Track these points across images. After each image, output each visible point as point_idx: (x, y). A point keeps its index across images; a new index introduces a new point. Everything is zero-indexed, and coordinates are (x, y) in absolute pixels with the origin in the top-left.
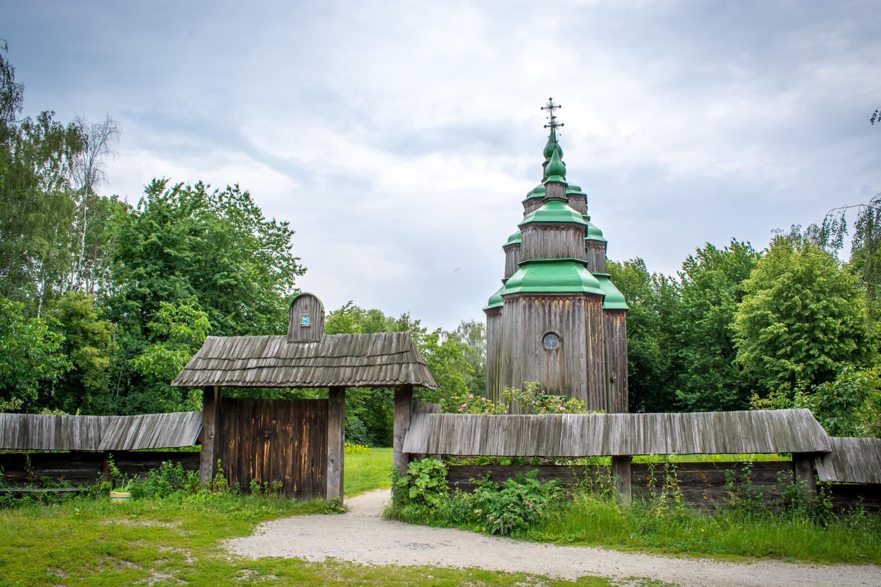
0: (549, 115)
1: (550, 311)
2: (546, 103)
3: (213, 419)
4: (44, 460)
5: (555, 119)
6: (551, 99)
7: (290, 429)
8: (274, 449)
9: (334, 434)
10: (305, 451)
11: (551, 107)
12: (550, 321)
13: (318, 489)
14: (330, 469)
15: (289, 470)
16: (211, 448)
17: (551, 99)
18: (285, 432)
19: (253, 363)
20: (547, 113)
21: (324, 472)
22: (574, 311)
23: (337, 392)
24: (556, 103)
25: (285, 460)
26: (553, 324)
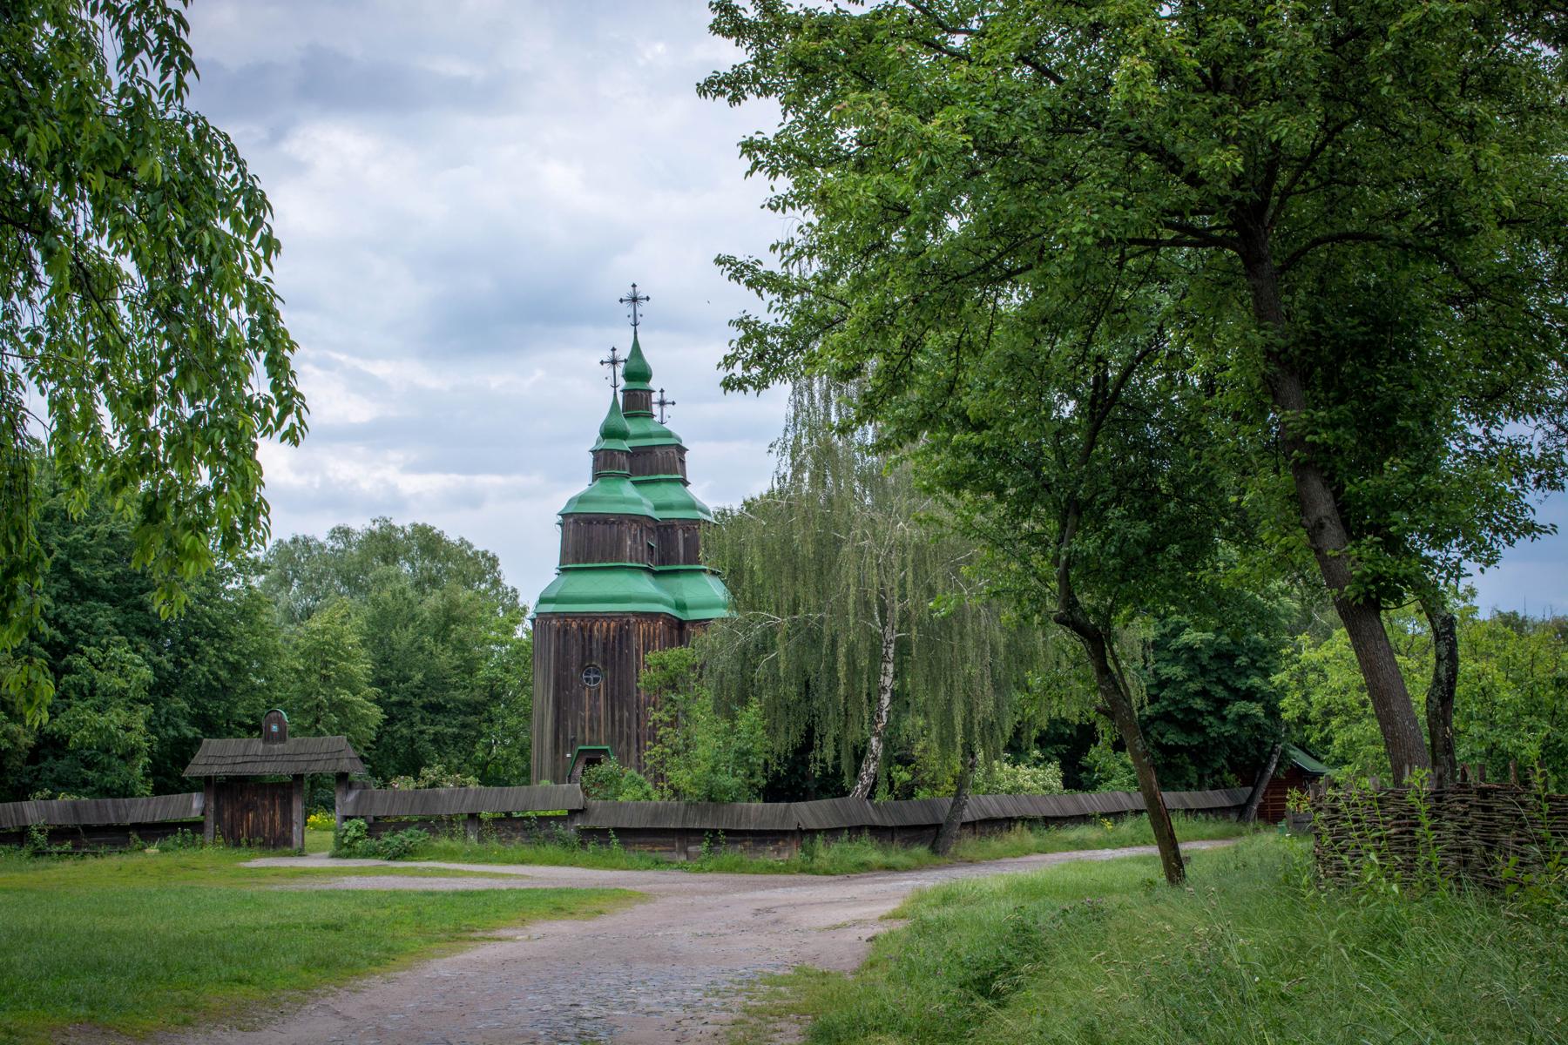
0: (631, 311)
1: (590, 636)
2: (626, 292)
3: (212, 797)
4: (90, 830)
5: (617, 353)
6: (634, 286)
7: (267, 803)
8: (256, 816)
9: (298, 807)
10: (278, 817)
11: (635, 300)
12: (591, 650)
13: (288, 842)
14: (295, 828)
15: (267, 830)
16: (212, 818)
17: (634, 286)
18: (264, 805)
19: (239, 760)
20: (627, 309)
21: (291, 831)
22: (621, 636)
23: (298, 778)
24: (642, 294)
25: (264, 823)
26: (595, 653)
